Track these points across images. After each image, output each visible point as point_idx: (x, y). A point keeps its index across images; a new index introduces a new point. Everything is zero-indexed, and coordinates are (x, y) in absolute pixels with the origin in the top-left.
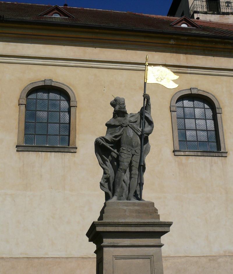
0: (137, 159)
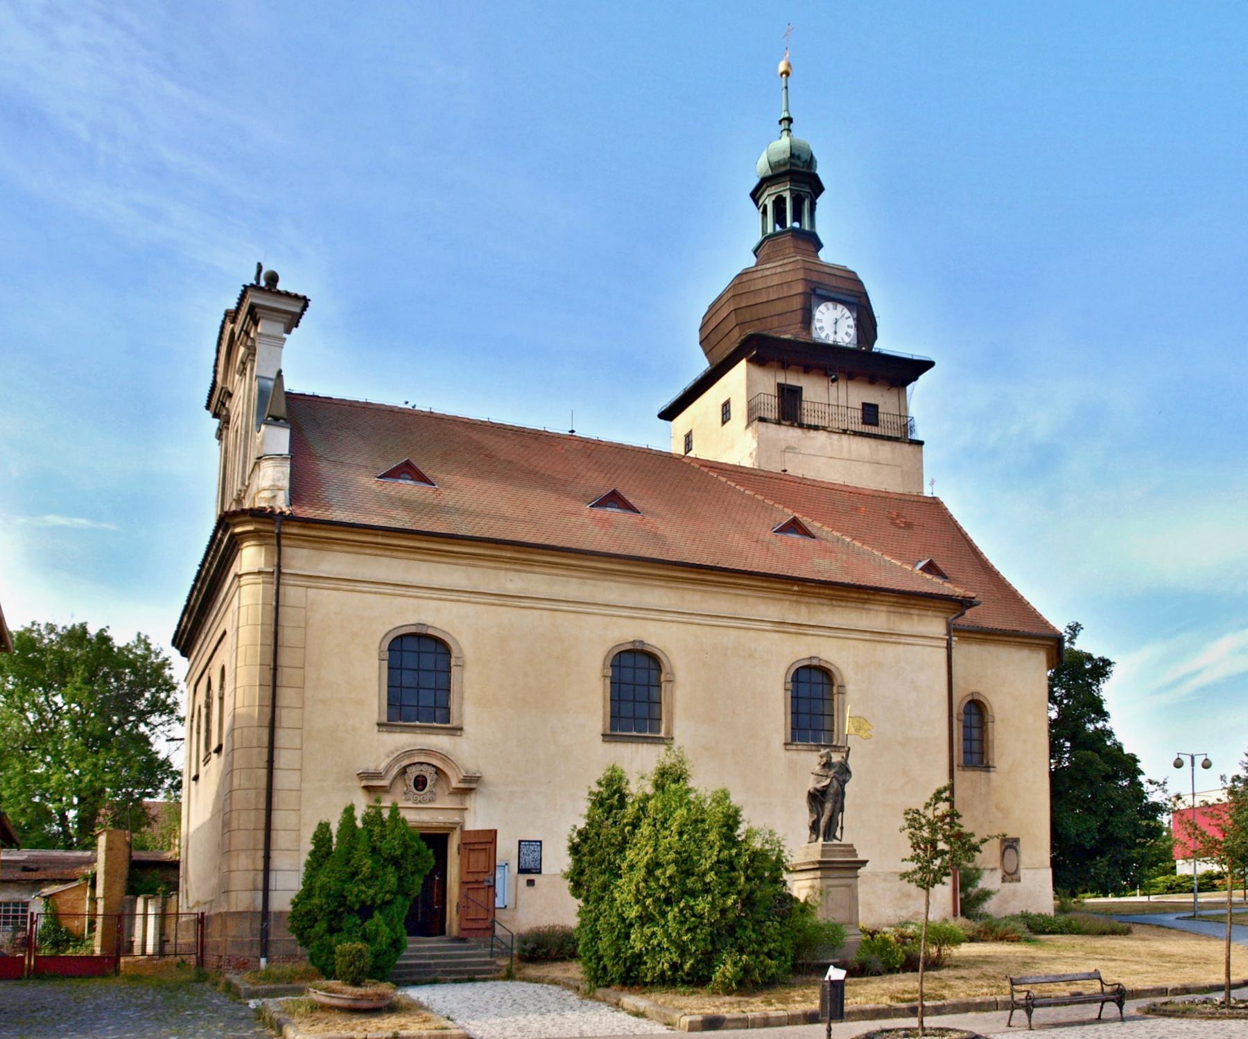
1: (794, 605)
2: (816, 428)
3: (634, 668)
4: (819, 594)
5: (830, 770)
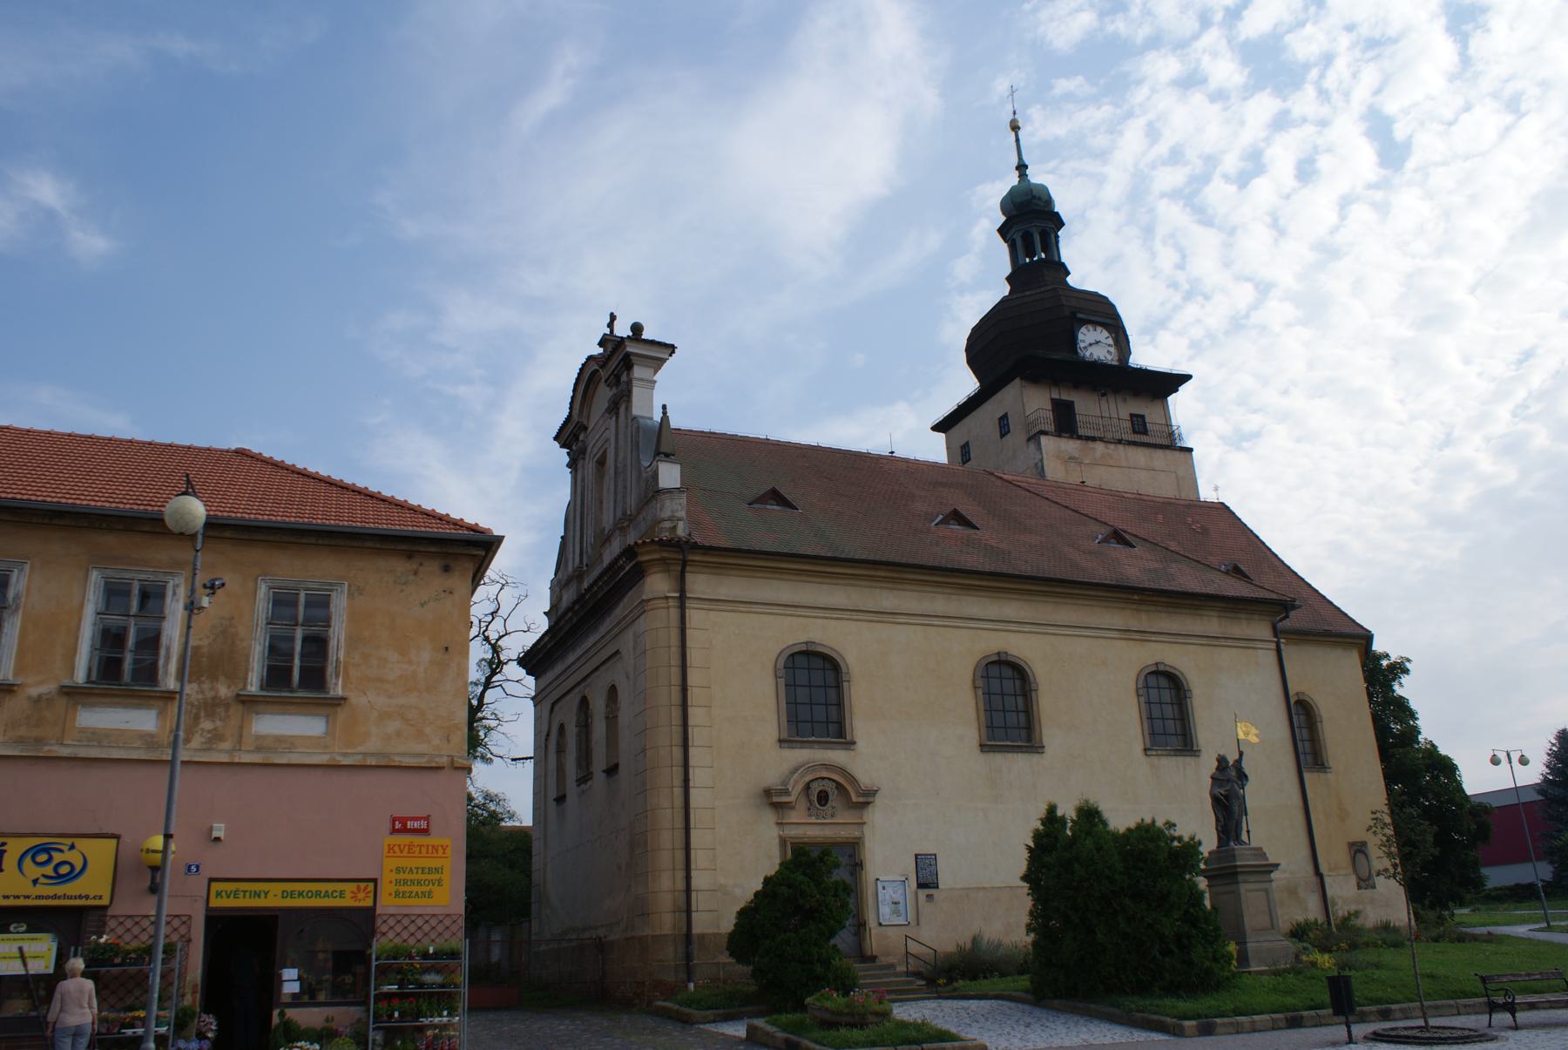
2: (1093, 439)
3: (1001, 678)
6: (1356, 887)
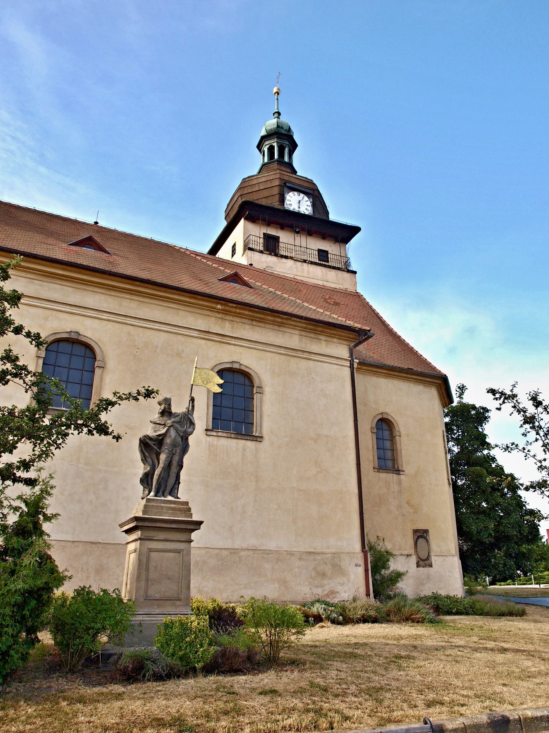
0: (176, 458)
1: (220, 320)
2: (286, 257)
4: (240, 313)
5: (170, 419)
6: (416, 565)
